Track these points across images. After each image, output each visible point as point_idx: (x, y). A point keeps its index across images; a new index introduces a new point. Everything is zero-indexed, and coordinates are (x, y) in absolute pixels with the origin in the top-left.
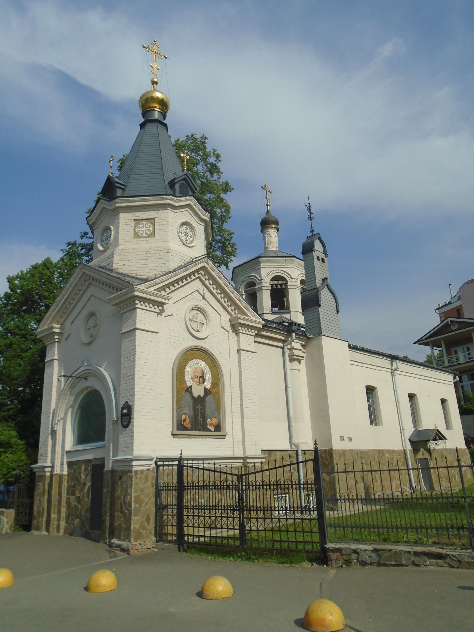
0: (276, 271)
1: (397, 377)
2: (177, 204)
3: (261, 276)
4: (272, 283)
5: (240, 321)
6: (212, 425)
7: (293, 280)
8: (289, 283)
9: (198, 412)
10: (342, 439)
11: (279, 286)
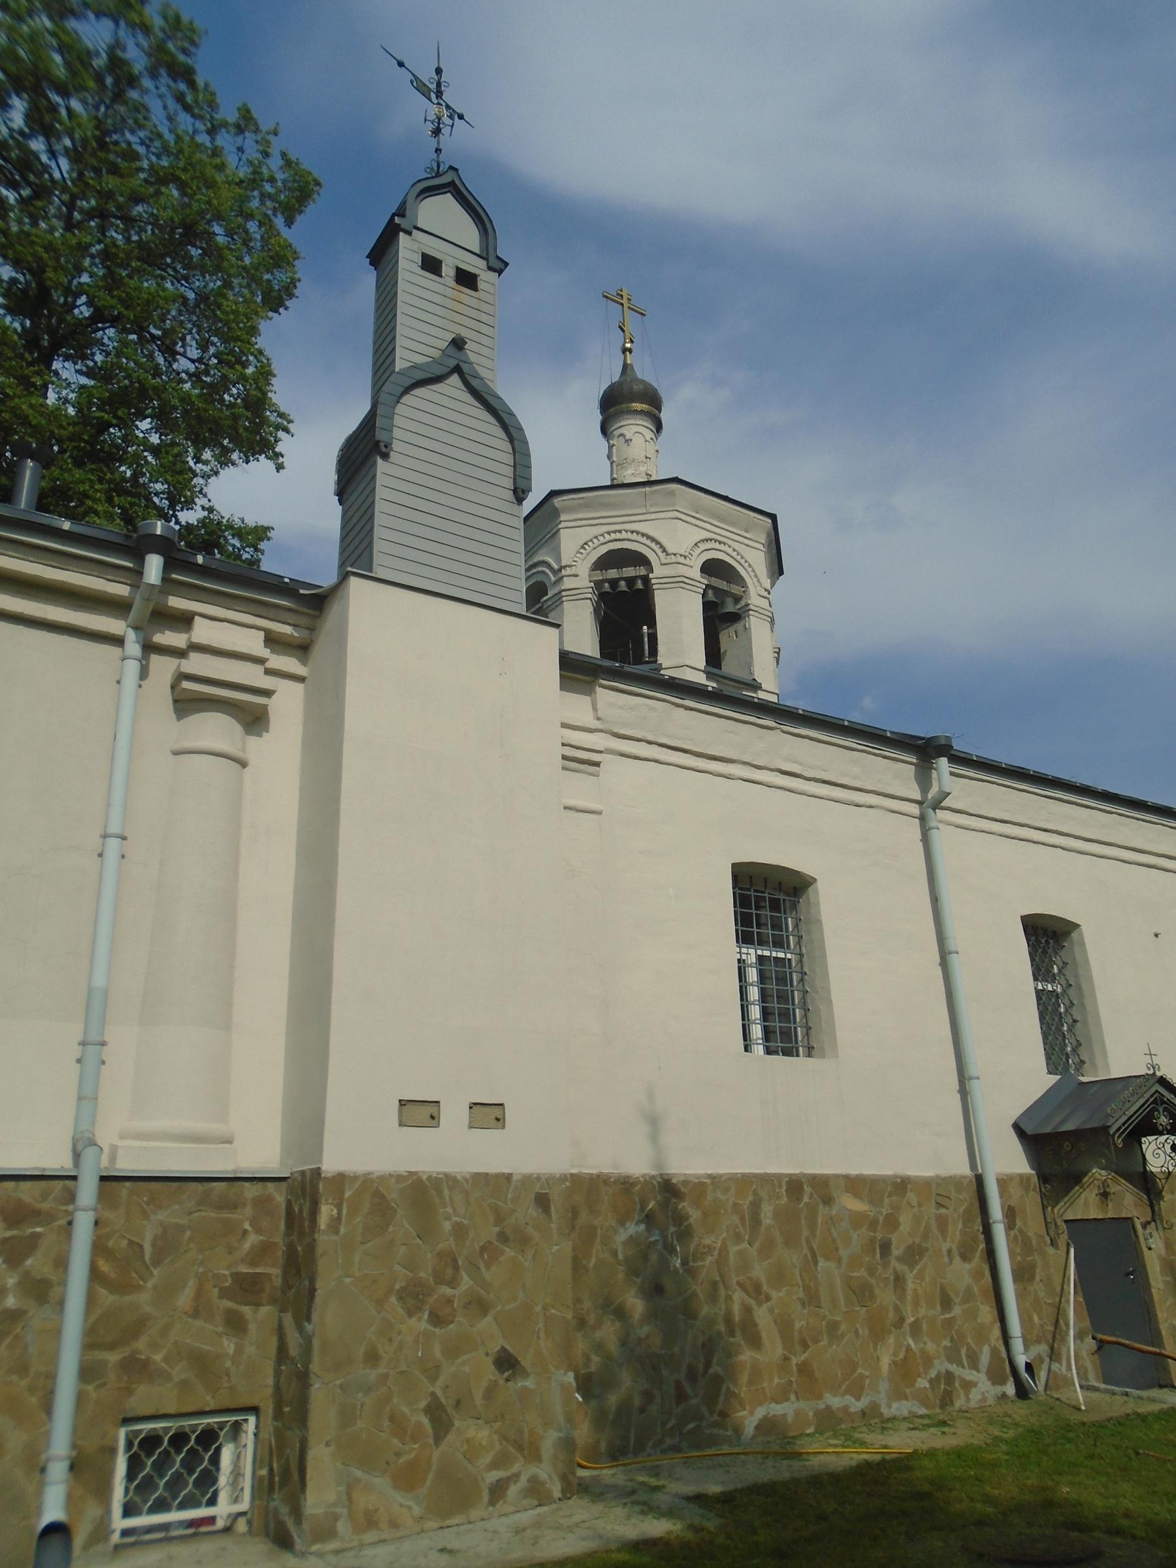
1: (942, 838)
3: (558, 559)
4: (598, 576)
7: (673, 559)
8: (658, 571)
10: (419, 1112)
11: (623, 585)
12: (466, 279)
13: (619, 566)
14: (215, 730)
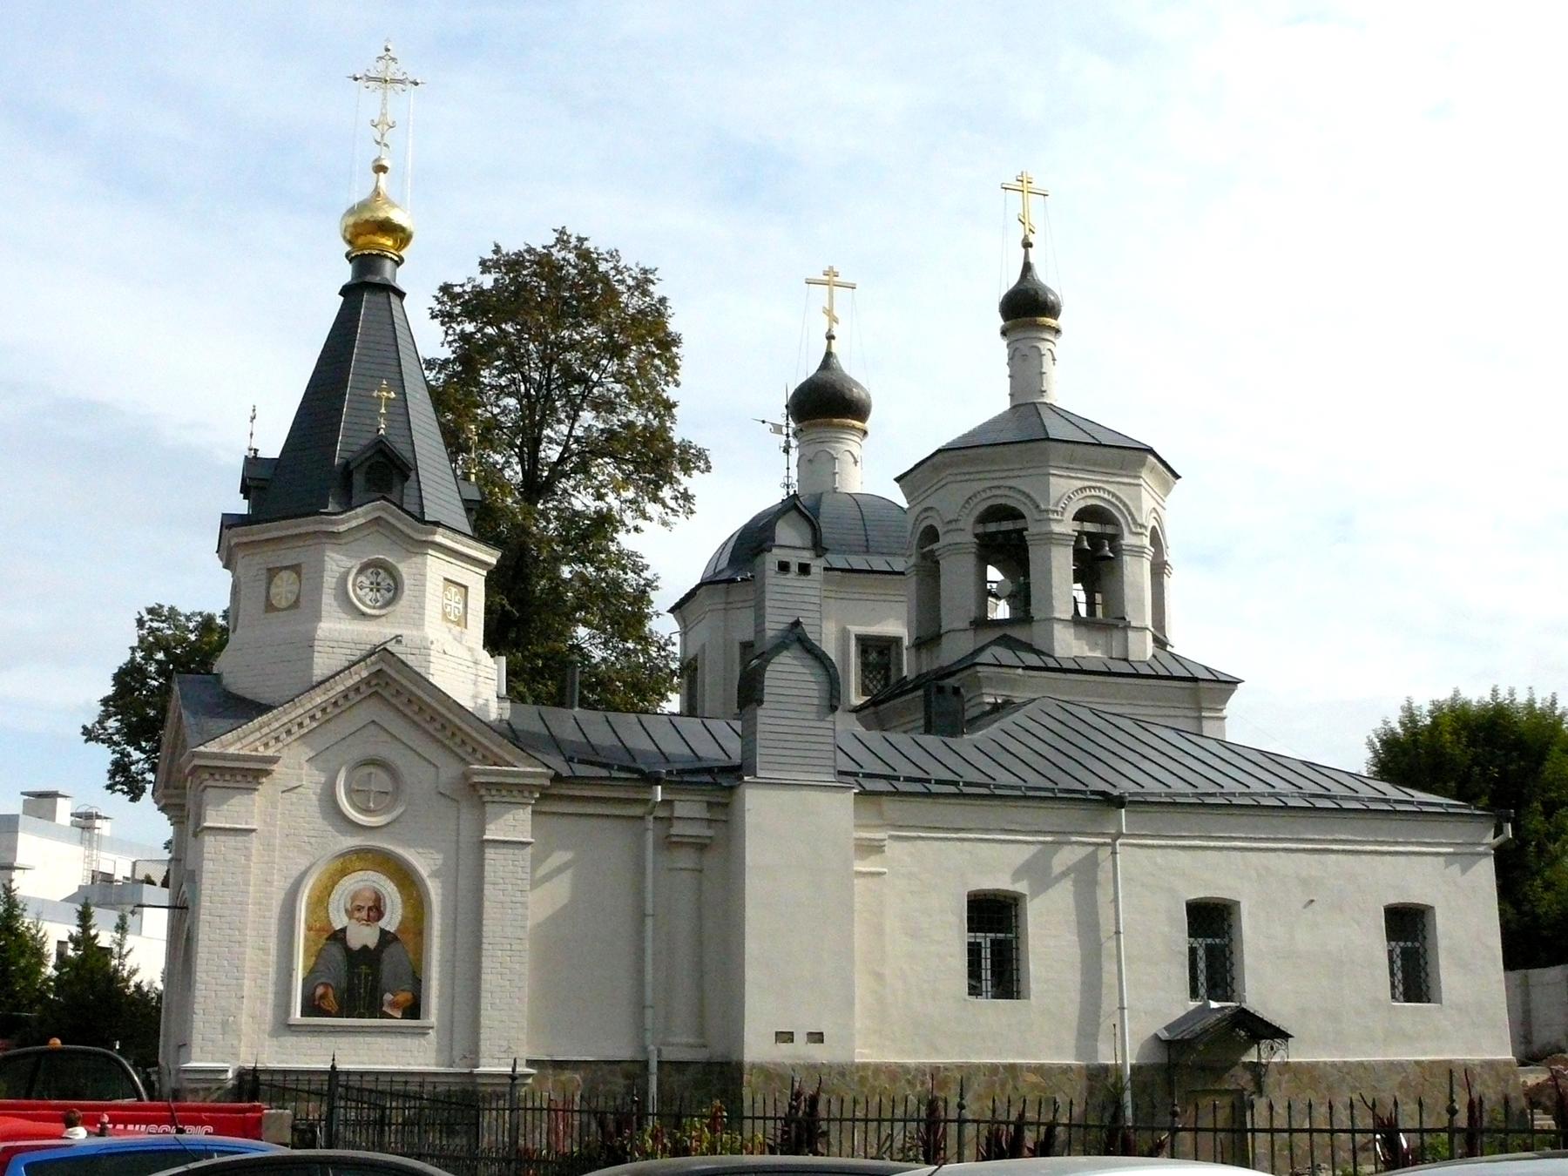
0: (989, 494)
2: (342, 528)
4: (980, 529)
5: (476, 779)
6: (394, 1005)
9: (360, 979)
10: (785, 1037)
12: (804, 569)
13: (999, 520)
14: (685, 859)
